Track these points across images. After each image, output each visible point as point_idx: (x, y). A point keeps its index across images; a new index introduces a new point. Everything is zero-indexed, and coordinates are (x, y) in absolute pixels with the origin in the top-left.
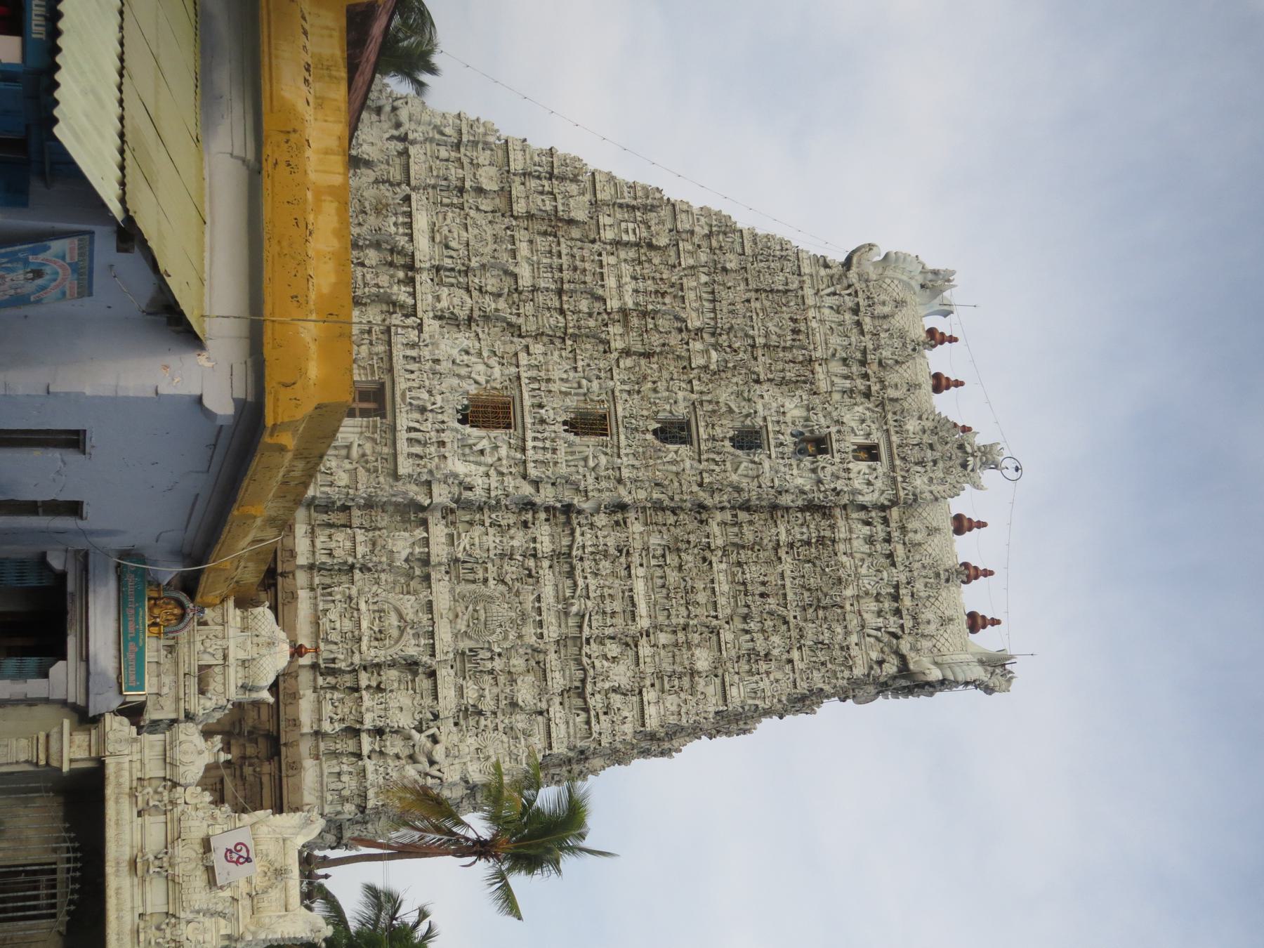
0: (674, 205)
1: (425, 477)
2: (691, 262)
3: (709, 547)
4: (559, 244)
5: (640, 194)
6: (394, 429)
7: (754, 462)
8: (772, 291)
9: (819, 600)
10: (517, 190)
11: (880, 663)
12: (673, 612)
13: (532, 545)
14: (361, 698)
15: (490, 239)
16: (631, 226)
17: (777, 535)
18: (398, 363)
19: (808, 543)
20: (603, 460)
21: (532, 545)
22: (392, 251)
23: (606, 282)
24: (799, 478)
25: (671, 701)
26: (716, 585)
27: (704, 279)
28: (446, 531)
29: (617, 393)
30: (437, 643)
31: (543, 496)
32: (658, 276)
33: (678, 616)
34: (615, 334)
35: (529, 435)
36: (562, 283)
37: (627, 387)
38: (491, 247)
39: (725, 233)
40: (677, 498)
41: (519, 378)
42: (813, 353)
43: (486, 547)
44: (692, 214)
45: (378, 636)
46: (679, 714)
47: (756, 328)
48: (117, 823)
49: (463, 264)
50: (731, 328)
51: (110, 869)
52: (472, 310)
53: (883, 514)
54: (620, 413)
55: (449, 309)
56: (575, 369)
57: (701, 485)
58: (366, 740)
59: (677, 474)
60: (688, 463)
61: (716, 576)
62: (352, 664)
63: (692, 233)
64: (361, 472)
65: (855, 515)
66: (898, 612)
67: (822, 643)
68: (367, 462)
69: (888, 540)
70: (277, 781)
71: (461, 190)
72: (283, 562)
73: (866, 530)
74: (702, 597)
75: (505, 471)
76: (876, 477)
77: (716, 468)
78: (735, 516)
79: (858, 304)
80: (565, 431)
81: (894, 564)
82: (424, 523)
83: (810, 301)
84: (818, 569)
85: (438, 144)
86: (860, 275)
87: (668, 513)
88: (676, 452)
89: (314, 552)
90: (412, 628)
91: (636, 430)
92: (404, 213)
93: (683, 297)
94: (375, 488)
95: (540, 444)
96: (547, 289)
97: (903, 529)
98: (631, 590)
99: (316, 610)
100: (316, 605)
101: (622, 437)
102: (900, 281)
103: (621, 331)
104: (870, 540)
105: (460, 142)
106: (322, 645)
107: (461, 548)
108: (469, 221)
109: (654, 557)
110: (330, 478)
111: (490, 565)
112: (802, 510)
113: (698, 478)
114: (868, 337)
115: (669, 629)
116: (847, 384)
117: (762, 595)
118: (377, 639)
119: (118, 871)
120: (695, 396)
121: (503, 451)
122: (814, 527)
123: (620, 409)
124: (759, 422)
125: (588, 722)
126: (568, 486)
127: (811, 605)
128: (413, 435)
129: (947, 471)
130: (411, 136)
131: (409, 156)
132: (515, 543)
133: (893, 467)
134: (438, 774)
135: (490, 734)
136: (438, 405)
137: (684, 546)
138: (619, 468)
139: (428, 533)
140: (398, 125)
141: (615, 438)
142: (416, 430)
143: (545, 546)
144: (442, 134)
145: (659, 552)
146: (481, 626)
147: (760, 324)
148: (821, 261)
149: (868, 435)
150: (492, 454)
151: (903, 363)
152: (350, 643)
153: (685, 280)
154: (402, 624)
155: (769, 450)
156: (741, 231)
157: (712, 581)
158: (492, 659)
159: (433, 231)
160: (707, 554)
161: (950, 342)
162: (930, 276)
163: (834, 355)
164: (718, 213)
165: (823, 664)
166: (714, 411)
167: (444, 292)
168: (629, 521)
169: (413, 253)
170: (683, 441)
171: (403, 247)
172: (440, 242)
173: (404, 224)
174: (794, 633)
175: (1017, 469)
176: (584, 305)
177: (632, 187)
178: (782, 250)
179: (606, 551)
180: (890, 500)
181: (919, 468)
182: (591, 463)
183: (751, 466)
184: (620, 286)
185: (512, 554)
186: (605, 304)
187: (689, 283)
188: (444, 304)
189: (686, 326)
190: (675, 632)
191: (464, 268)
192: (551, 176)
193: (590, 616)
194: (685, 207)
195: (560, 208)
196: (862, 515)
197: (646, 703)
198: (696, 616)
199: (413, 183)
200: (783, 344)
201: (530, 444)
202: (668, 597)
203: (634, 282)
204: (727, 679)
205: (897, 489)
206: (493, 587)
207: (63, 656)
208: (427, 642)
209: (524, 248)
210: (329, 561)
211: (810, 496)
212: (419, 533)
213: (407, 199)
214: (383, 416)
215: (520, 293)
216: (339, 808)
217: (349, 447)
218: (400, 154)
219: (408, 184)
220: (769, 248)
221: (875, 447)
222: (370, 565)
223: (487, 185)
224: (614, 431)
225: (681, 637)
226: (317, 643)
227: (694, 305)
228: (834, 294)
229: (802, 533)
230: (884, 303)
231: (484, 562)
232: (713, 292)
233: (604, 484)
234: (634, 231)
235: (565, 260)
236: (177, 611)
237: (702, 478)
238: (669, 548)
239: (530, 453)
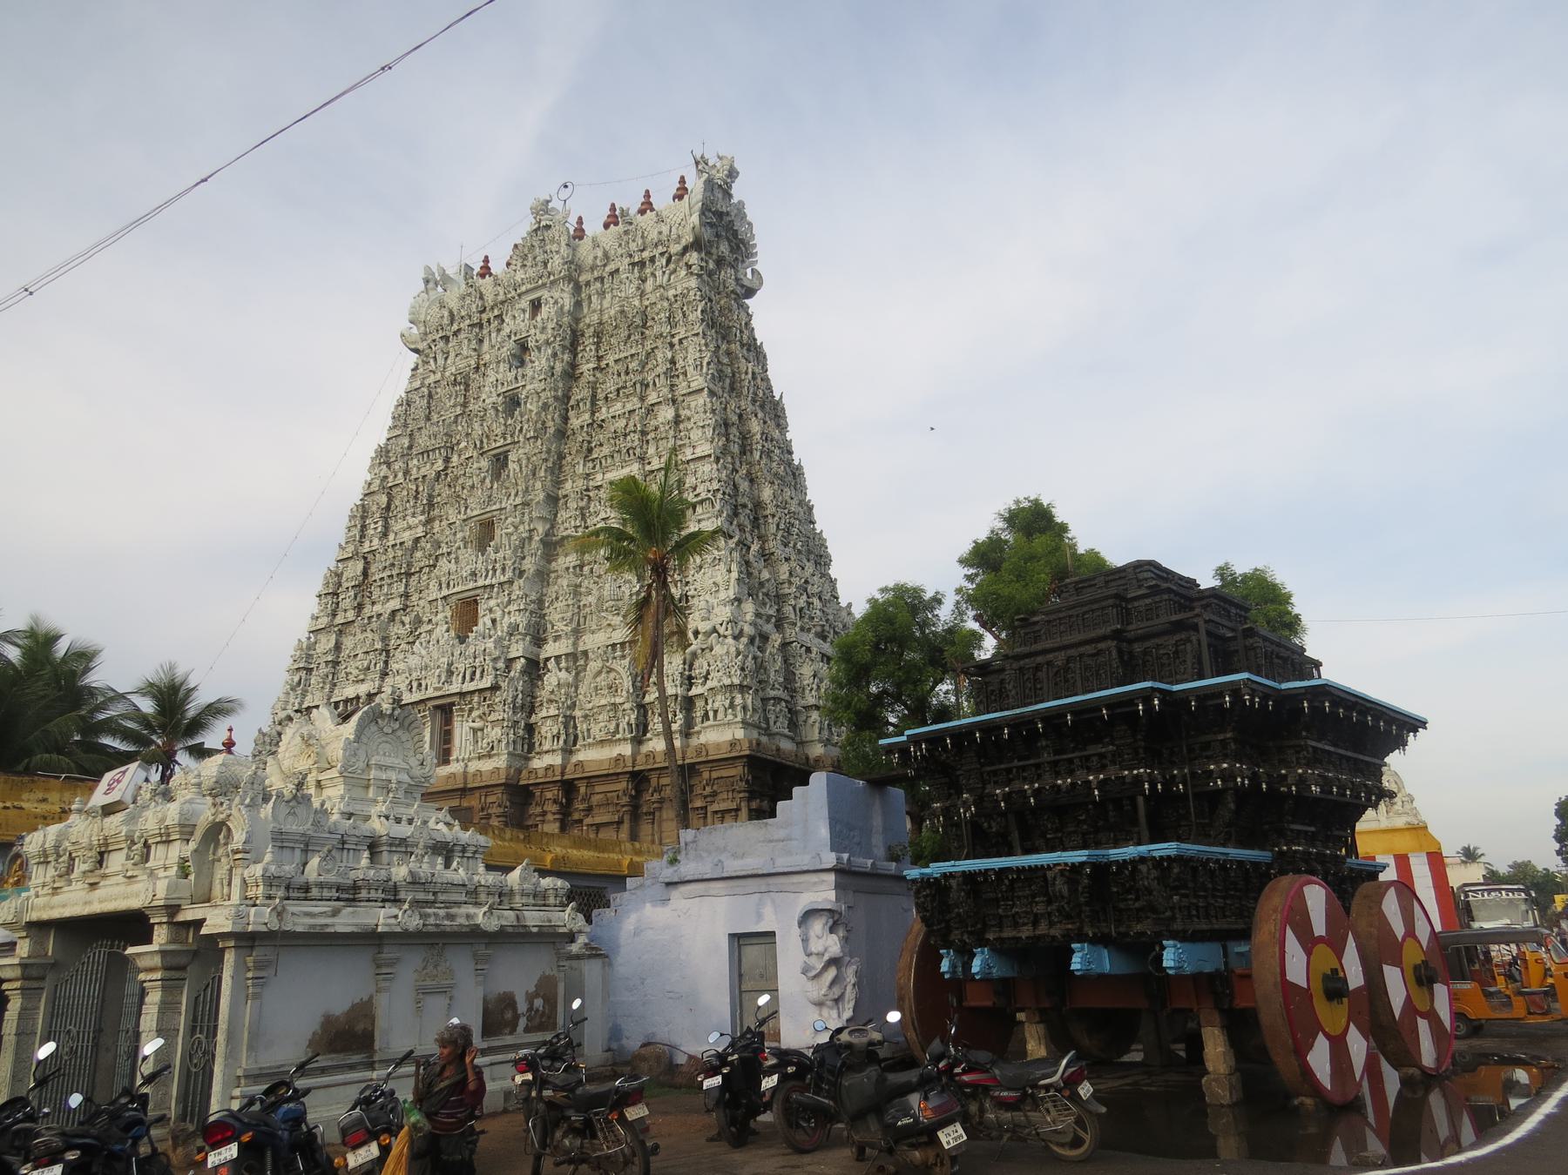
0: (366, 495)
1: (501, 665)
2: (400, 475)
3: (592, 424)
4: (375, 581)
6: (462, 694)
7: (527, 397)
8: (429, 407)
9: (637, 326)
10: (339, 619)
11: (689, 267)
12: (629, 445)
13: (571, 570)
16: (372, 526)
18: (416, 697)
19: (598, 344)
20: (510, 520)
21: (571, 570)
24: (539, 362)
25: (696, 434)
26: (617, 413)
29: (465, 517)
31: (529, 566)
32: (406, 499)
33: (633, 441)
35: (481, 583)
36: (401, 574)
37: (463, 509)
38: (369, 635)
39: (388, 452)
40: (544, 456)
41: (445, 598)
43: (565, 608)
46: (703, 427)
48: (64, 906)
49: (380, 654)
50: (446, 434)
56: (449, 554)
57: (536, 438)
59: (528, 459)
60: (521, 451)
61: (610, 416)
62: (631, 709)
63: (386, 477)
64: (489, 719)
65: (585, 310)
66: (652, 260)
67: (669, 318)
68: (484, 714)
69: (601, 279)
70: (715, 764)
72: (537, 778)
73: (594, 298)
74: (622, 423)
78: (572, 407)
79: (441, 338)
81: (617, 271)
83: (438, 376)
84: (615, 332)
86: (423, 340)
87: (564, 462)
89: (553, 751)
90: (608, 661)
91: (490, 497)
94: (505, 705)
95: (491, 572)
96: (406, 586)
97: (593, 269)
99: (593, 744)
100: (589, 744)
101: (494, 507)
102: (429, 307)
103: (437, 522)
104: (602, 294)
105: (304, 668)
106: (618, 736)
107: (565, 628)
109: (594, 468)
111: (582, 604)
112: (575, 355)
113: (532, 441)
114: (462, 325)
115: (645, 446)
117: (627, 373)
118: (617, 691)
120: (475, 454)
121: (492, 603)
122: (588, 341)
123: (475, 513)
125: (701, 502)
126: (526, 546)
127: (642, 333)
128: (468, 678)
129: (552, 241)
132: (565, 583)
133: (544, 285)
135: (697, 585)
138: (515, 506)
141: (495, 513)
142: (464, 677)
144: (299, 683)
145: (590, 465)
146: (620, 603)
148: (414, 373)
149: (524, 311)
150: (495, 612)
151: (481, 294)
156: (388, 439)
157: (613, 417)
159: (357, 682)
161: (488, 262)
162: (431, 285)
163: (475, 350)
164: (373, 459)
165: (684, 315)
166: (487, 437)
168: (564, 493)
170: (506, 458)
172: (365, 675)
174: (659, 343)
175: (566, 187)
176: (419, 554)
177: (349, 529)
178: (402, 405)
179: (582, 508)
180: (569, 283)
181: (549, 265)
182: (511, 530)
183: (530, 401)
184: (410, 528)
185: (576, 586)
190: (648, 442)
192: (336, 594)
195: (353, 583)
196: (585, 304)
197: (693, 457)
198: (635, 425)
200: (463, 392)
201: (488, 582)
202: (619, 451)
203: (408, 518)
204: (684, 392)
205: (559, 279)
208: (628, 648)
209: (377, 608)
210: (563, 737)
211: (557, 347)
212: (551, 664)
214: (453, 704)
215: (407, 606)
216: (739, 708)
217: (475, 731)
221: (532, 302)
222: (569, 702)
224: (490, 515)
225: (652, 435)
226: (616, 741)
227: (428, 467)
228: (435, 358)
229: (591, 350)
230: (442, 317)
231: (579, 607)
232: (422, 453)
233: (526, 517)
234: (376, 523)
235: (384, 575)
237: (531, 438)
238: (586, 457)
239: (494, 581)
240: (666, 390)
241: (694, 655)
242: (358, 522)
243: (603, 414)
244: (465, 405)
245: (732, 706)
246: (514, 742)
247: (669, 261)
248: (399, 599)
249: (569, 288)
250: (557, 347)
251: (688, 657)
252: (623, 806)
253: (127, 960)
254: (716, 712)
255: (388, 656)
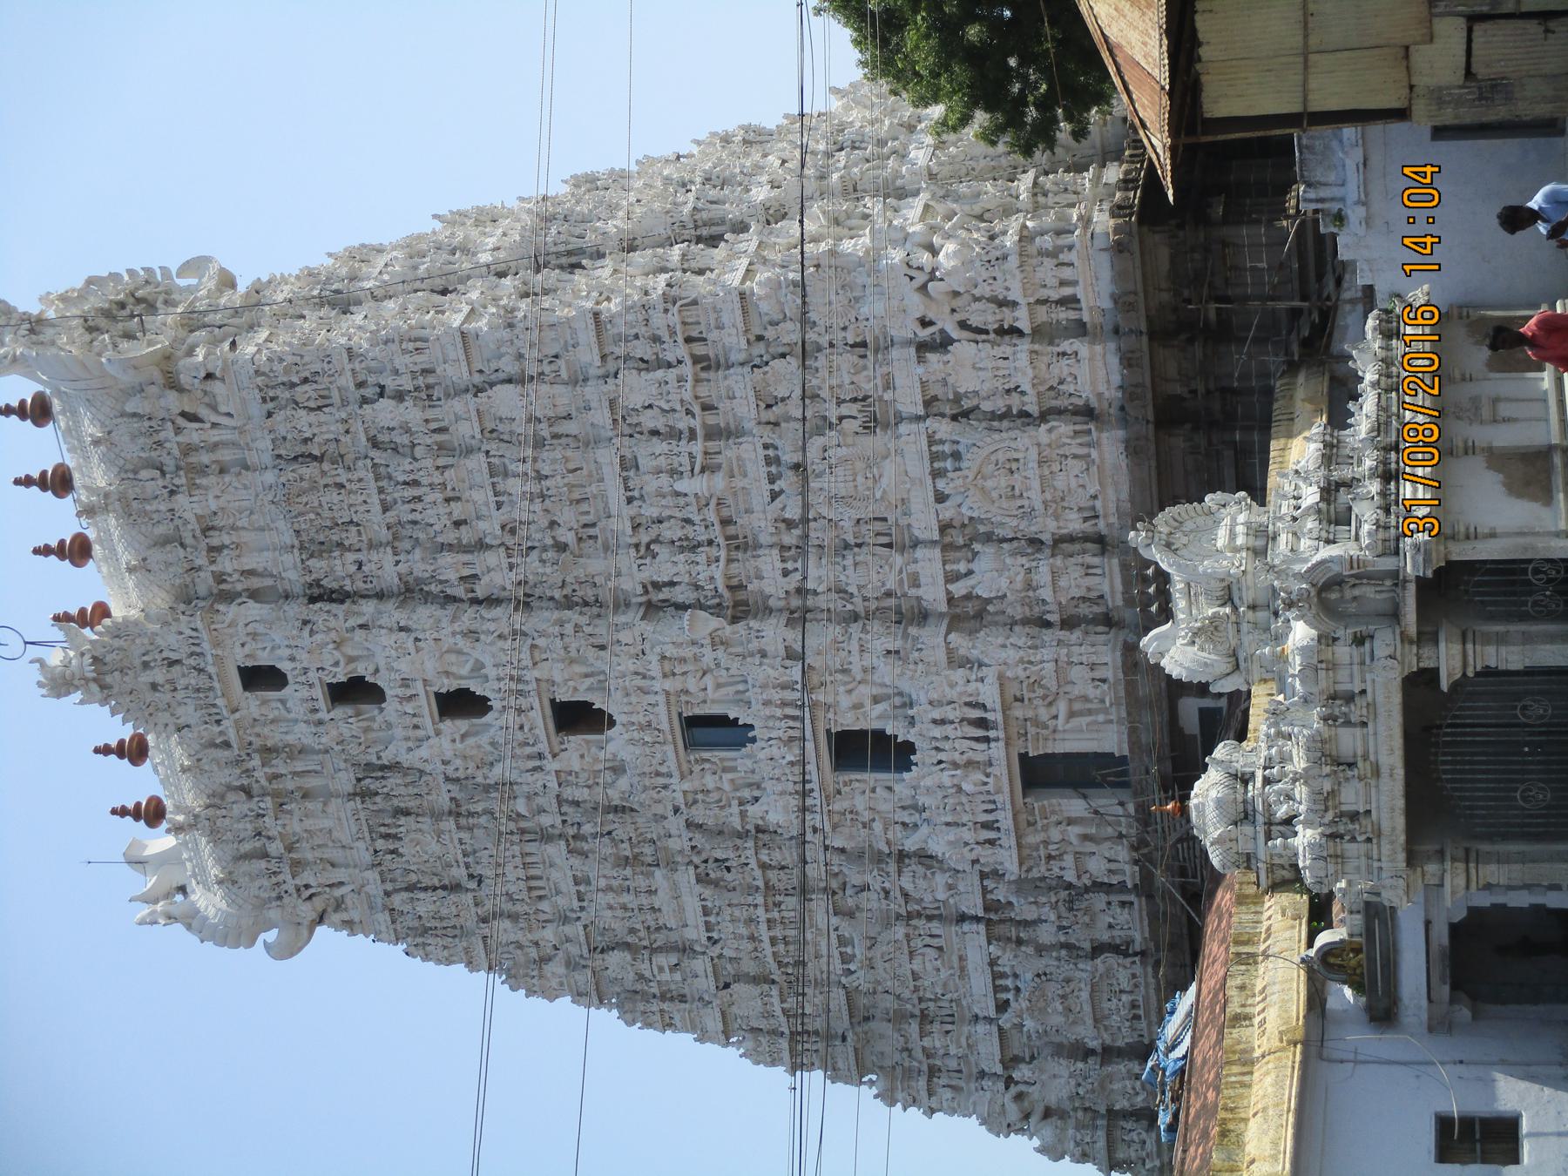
2: (568, 930)
4: (774, 953)
5: (657, 1017)
7: (447, 674)
14: (1034, 385)
15: (879, 964)
16: (666, 976)
17: (397, 563)
22: (1019, 942)
23: (698, 905)
26: (492, 499)
27: (544, 906)
28: (920, 592)
29: (676, 774)
30: (925, 448)
34: (680, 836)
36: (766, 905)
40: (569, 629)
42: (360, 807)
43: (860, 569)
44: (571, 991)
45: (1014, 466)
47: (456, 841)
49: (916, 928)
51: (1400, 772)
52: (900, 872)
53: (223, 586)
54: (669, 749)
55: (933, 874)
58: (1024, 325)
64: (1052, 685)
65: (269, 582)
71: (924, 1018)
75: (839, 676)
76: (243, 645)
77: (514, 673)
80: (751, 727)
82: (951, 600)
83: (372, 875)
85: (960, 1071)
88: (575, 689)
92: (1006, 989)
93: (576, 884)
98: (630, 500)
101: (664, 718)
108: (912, 983)
110: (1097, 674)
116: (299, 766)
118: (1017, 460)
119: (1391, 770)
121: (845, 701)
122: (338, 569)
124: (448, 725)
130: (1001, 1085)
131: (1002, 1061)
134: (913, 273)
136: (946, 773)
137: (550, 555)
138: (665, 676)
139: (948, 592)
140: (1019, 1097)
143: (769, 563)
147: (450, 845)
152: (1054, 456)
153: (576, 904)
154: (980, 482)
155: (426, 692)
158: (841, 419)
159: (962, 969)
160: (509, 541)
164: (530, 993)
167: (941, 896)
168: (640, 590)
169: (989, 943)
171: (1004, 950)
173: (1003, 975)
181: (174, 656)
186: (697, 875)
187: (567, 901)
188: (941, 879)
189: (568, 845)
190: (556, 436)
191: (913, 922)
193: (692, 470)
194: (585, 1000)
196: (255, 583)
199: (995, 1029)
204: (465, 369)
206: (846, 518)
207: (1454, 929)
213: (1002, 1006)
217: (1072, 714)
218: (1017, 1060)
219: (1000, 1029)
220: (445, 947)
223: (887, 1029)
232: (530, 889)
234: (661, 969)
235: (765, 937)
236: (1332, 960)
240: (457, 405)
241: (963, 325)
242: (655, 1006)
243: (490, 527)
244: (437, 816)
245: (1053, 254)
246: (1093, 645)
247: (193, 418)
248: (813, 905)
249: (231, 611)
250: (352, 622)
251: (966, 334)
252: (1210, 443)
253: (1455, 686)
254: (1063, 283)
255: (919, 915)
